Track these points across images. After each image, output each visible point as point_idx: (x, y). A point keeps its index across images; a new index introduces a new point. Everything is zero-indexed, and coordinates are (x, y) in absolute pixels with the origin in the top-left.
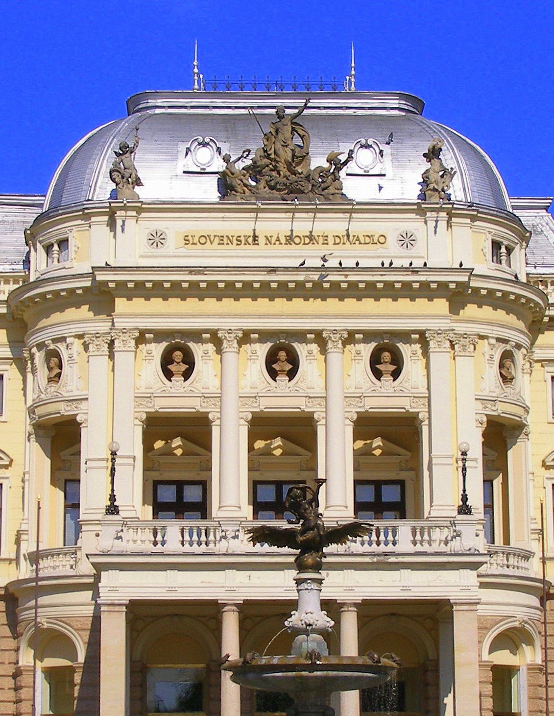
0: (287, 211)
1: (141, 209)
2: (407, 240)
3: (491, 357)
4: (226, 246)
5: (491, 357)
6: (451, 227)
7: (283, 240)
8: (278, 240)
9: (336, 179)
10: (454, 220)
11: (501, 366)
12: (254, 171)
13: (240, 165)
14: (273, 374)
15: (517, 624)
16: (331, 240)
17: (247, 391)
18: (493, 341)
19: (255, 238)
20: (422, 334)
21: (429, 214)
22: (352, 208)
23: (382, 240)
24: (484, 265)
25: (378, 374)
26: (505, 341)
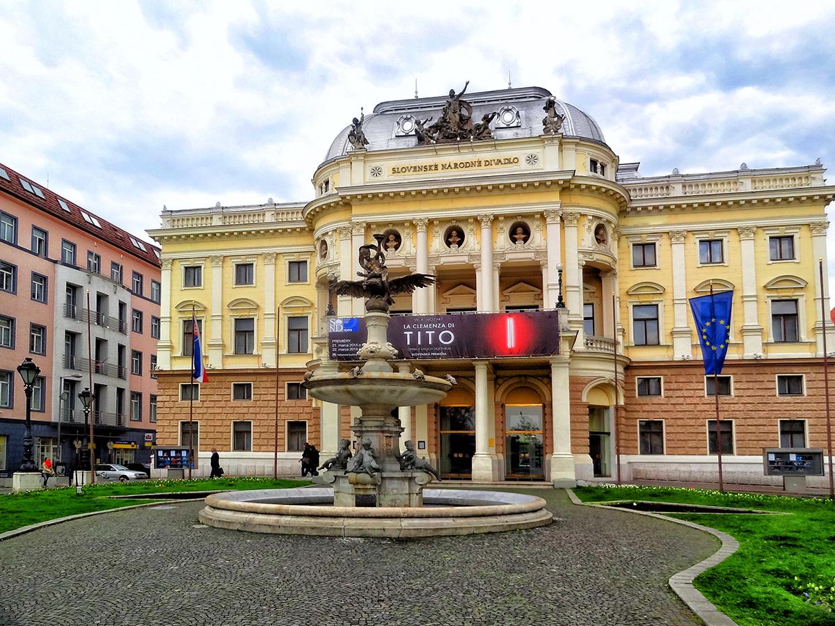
0: (455, 149)
1: (368, 155)
2: (532, 159)
3: (589, 227)
4: (419, 173)
5: (589, 227)
6: (562, 151)
7: (453, 166)
8: (449, 166)
9: (486, 128)
10: (564, 146)
11: (597, 233)
12: (436, 127)
13: (426, 126)
14: (449, 244)
15: (606, 382)
16: (483, 164)
17: (433, 253)
18: (591, 217)
19: (436, 166)
20: (542, 214)
21: (546, 143)
22: (497, 144)
23: (516, 160)
24: (584, 170)
25: (514, 240)
26: (600, 218)
